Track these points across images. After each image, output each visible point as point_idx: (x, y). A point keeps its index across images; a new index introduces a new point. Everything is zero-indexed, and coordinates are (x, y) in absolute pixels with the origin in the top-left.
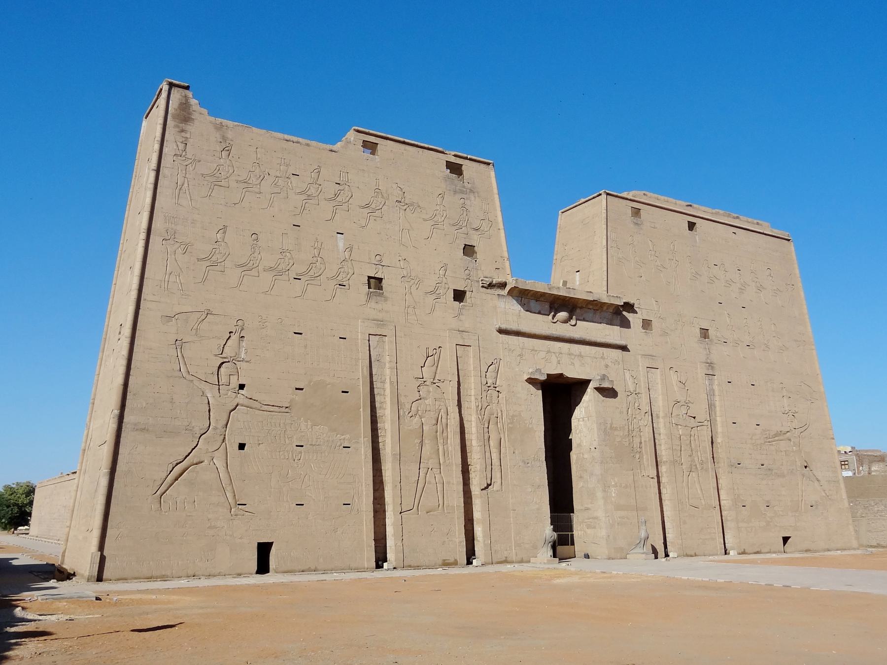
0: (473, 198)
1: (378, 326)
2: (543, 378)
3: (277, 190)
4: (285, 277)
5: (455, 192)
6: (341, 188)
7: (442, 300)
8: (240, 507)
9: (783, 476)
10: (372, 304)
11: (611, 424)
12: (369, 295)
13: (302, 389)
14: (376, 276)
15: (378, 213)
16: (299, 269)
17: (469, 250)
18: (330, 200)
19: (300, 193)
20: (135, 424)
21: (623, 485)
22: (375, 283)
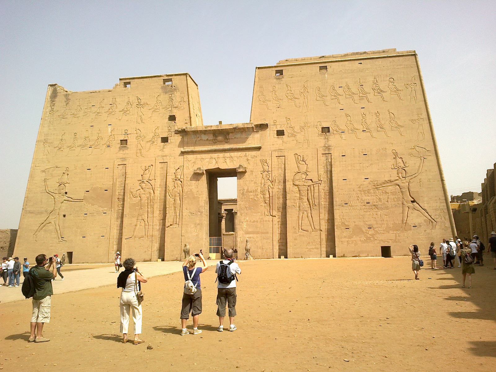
0: (176, 93)
1: (122, 161)
2: (201, 172)
3: (86, 114)
4: (86, 148)
5: (166, 93)
6: (112, 105)
7: (155, 143)
8: (62, 238)
9: (387, 208)
10: (121, 152)
11: (248, 189)
12: (120, 148)
13: (89, 191)
16: (91, 143)
17: (172, 118)
18: (107, 112)
19: (95, 113)
20: (30, 211)
21: (252, 221)
22: (124, 142)
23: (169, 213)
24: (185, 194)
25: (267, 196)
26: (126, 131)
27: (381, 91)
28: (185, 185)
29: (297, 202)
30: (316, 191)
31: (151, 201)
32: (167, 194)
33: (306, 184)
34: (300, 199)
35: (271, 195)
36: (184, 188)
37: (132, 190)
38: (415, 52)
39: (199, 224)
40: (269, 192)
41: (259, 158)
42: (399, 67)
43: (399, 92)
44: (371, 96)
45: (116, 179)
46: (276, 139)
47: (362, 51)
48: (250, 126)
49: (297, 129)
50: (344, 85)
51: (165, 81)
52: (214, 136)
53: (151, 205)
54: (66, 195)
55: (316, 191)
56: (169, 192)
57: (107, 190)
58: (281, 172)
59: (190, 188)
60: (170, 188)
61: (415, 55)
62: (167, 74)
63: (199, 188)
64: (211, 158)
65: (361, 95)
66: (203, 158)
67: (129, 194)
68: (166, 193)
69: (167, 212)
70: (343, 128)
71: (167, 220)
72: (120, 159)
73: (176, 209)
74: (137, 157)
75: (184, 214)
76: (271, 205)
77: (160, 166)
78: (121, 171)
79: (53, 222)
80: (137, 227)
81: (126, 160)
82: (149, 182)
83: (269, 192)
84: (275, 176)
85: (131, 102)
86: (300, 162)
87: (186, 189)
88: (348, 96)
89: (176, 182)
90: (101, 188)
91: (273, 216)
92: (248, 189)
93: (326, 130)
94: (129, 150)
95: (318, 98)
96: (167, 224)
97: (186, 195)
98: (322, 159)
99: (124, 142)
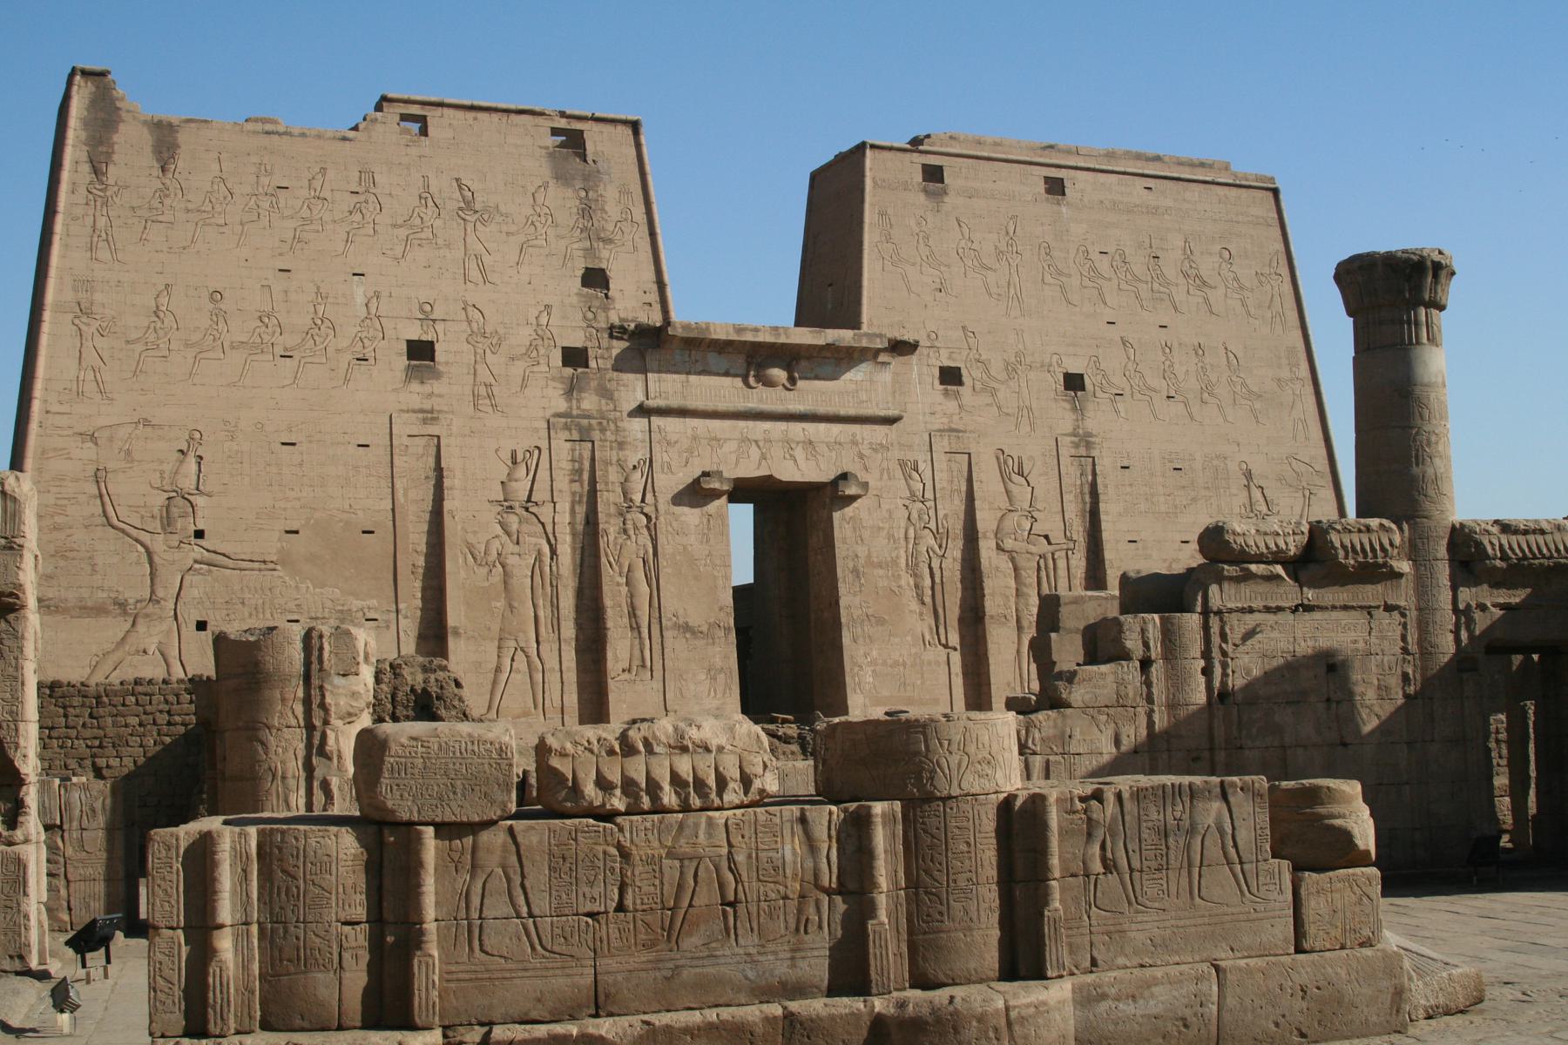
1: (425, 421)
2: (726, 488)
6: (362, 198)
10: (415, 386)
11: (869, 556)
14: (424, 338)
15: (427, 234)
16: (290, 340)
17: (595, 279)
22: (421, 351)
25: (928, 582)
26: (428, 308)
27: (1204, 283)
29: (1013, 600)
30: (1062, 572)
32: (604, 559)
33: (1033, 549)
34: (1018, 593)
35: (938, 580)
36: (662, 540)
37: (471, 538)
38: (1272, 180)
40: (930, 568)
41: (896, 454)
42: (1240, 218)
43: (1247, 294)
44: (1179, 295)
45: (406, 490)
46: (939, 398)
47: (1151, 151)
48: (879, 344)
49: (997, 368)
50: (1111, 249)
51: (555, 132)
52: (749, 364)
53: (545, 594)
54: (199, 541)
55: (1062, 572)
58: (959, 505)
60: (611, 538)
61: (1275, 192)
62: (568, 112)
63: (712, 542)
64: (745, 440)
65: (1156, 286)
68: (597, 557)
69: (610, 624)
70: (1119, 381)
71: (610, 655)
72: (414, 411)
73: (638, 613)
76: (940, 611)
79: (152, 648)
83: (930, 568)
84: (946, 516)
85: (436, 196)
86: (1016, 478)
88: (1124, 286)
89: (629, 516)
91: (946, 646)
92: (869, 556)
93: (1074, 382)
94: (445, 380)
95: (1048, 279)
98: (1071, 472)
99: (421, 351)
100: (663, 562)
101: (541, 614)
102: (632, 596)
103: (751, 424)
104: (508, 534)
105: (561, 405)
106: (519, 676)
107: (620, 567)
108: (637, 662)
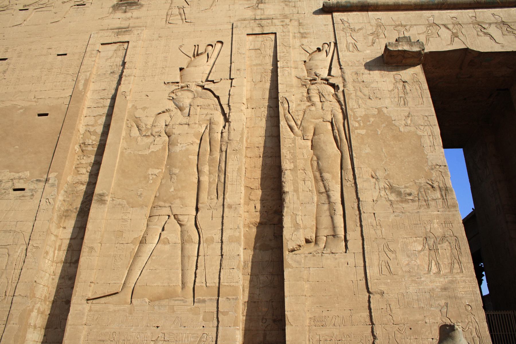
1: (118, 34)
10: (119, 14)
23: (296, 191)
24: (357, 125)
28: (353, 96)
31: (215, 149)
36: (351, 104)
39: (444, 238)
53: (211, 161)
56: (289, 116)
57: (47, 115)
59: (379, 104)
60: (293, 106)
63: (410, 104)
66: (404, 23)
67: (124, 126)
69: (288, 187)
73: (326, 175)
74: (170, 25)
75: (365, 196)
77: (245, 44)
78: (107, 60)
80: (149, 248)
81: (131, 30)
82: (205, 87)
87: (357, 108)
90: (26, 109)
94: (144, 9)
96: (291, 236)
97: (363, 129)
100: (353, 123)
101: (205, 179)
102: (318, 159)
103: (436, 13)
104: (181, 109)
105: (249, 14)
106: (167, 247)
107: (304, 130)
108: (324, 232)
